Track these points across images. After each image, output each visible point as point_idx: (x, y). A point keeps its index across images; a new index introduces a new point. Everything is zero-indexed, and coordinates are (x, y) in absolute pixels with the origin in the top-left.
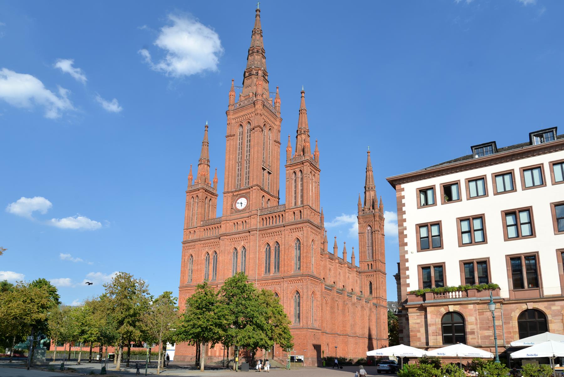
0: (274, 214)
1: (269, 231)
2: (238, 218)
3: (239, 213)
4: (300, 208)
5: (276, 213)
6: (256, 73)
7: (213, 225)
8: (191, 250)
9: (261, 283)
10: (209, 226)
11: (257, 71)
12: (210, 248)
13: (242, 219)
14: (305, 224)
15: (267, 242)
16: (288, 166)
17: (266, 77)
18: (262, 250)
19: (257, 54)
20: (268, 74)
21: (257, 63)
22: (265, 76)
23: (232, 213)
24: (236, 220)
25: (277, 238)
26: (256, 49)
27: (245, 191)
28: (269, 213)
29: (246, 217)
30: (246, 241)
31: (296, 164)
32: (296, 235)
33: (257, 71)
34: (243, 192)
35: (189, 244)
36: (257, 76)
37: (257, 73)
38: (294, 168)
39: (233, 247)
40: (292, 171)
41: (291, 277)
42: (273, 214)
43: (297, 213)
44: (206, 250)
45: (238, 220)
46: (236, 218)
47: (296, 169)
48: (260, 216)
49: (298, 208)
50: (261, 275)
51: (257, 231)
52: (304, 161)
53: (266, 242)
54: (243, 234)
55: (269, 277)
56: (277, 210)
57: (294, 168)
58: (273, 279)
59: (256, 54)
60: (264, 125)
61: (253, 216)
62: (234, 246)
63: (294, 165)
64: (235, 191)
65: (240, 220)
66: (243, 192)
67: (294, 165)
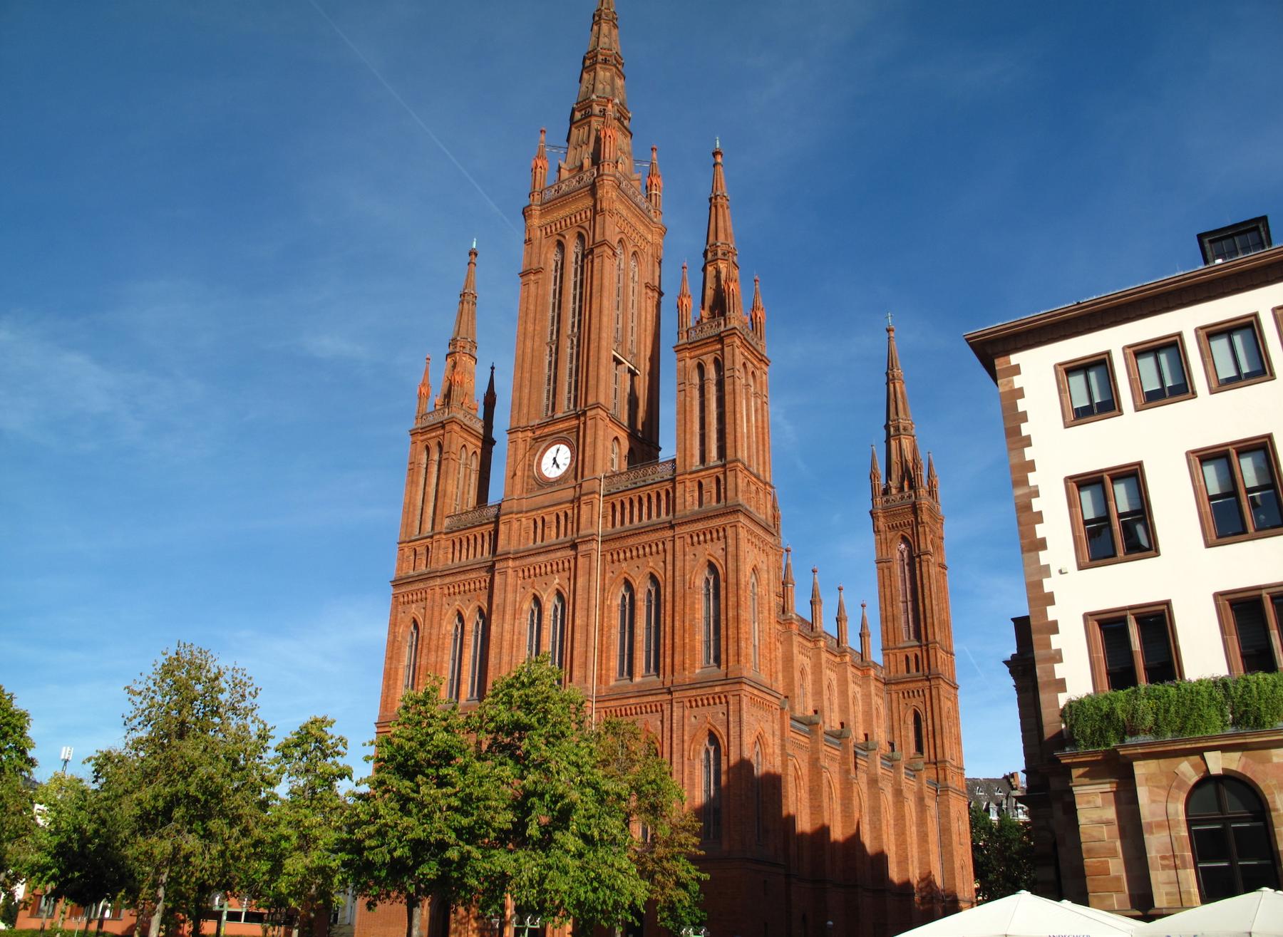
0: (644, 488)
1: (631, 542)
2: (547, 504)
3: (549, 490)
4: (716, 470)
5: (650, 487)
6: (600, 111)
7: (477, 529)
8: (414, 606)
9: (608, 708)
10: (467, 531)
11: (602, 108)
12: (468, 596)
13: (555, 508)
14: (732, 518)
15: (626, 576)
16: (681, 348)
17: (626, 123)
18: (611, 602)
19: (604, 66)
20: (630, 115)
21: (604, 89)
22: (622, 119)
24: (539, 512)
25: (654, 564)
26: (602, 55)
27: (567, 424)
28: (630, 486)
29: (567, 502)
31: (705, 342)
32: (707, 553)
33: (602, 108)
34: (561, 426)
35: (410, 588)
36: (603, 119)
37: (603, 113)
38: (698, 352)
40: (695, 362)
41: (693, 686)
42: (641, 489)
43: (710, 485)
44: (457, 603)
45: (545, 510)
46: (540, 505)
47: (704, 357)
48: (607, 498)
49: (712, 471)
50: (607, 682)
51: (598, 541)
52: (726, 334)
53: (622, 577)
54: (559, 554)
55: (630, 689)
56: (652, 477)
57: (698, 352)
58: (641, 694)
59: (601, 68)
60: (620, 241)
62: (533, 591)
63: (698, 344)
64: (540, 426)
65: (551, 509)
66: (561, 426)
67: (698, 344)
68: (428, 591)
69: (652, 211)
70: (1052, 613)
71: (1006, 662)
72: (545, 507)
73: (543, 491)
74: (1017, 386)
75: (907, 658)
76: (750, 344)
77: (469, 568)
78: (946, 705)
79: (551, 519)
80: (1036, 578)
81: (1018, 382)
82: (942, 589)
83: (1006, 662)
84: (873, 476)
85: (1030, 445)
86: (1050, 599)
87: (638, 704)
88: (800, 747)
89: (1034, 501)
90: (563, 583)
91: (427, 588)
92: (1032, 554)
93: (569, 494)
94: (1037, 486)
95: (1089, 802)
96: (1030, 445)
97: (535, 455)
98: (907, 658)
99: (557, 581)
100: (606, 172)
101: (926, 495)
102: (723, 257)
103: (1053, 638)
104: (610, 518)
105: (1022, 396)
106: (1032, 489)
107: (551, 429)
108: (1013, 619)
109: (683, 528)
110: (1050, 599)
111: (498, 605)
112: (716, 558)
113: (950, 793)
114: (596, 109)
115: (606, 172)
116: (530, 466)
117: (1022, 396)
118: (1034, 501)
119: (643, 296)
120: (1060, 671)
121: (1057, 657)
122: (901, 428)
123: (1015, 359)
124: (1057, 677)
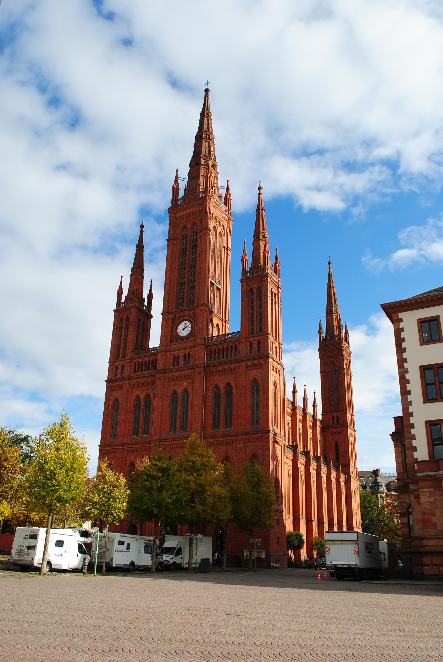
5: (228, 343)
6: (204, 163)
13: (184, 350)
16: (243, 281)
23: (172, 342)
24: (177, 352)
29: (190, 348)
30: (190, 381)
39: (172, 389)
42: (224, 344)
44: (138, 392)
45: (179, 351)
47: (254, 285)
61: (199, 347)
62: (174, 388)
65: (183, 351)
68: (124, 385)
69: (227, 211)
70: (412, 420)
71: (390, 435)
72: (180, 350)
73: (178, 342)
74: (401, 327)
75: (333, 417)
76: (274, 280)
77: (143, 376)
78: (350, 439)
79: (181, 355)
80: (406, 406)
81: (401, 325)
82: (350, 386)
83: (390, 435)
84: (320, 332)
85: (405, 352)
86: (411, 414)
87: (222, 440)
88: (290, 459)
89: (406, 375)
90: (188, 385)
91: (123, 384)
92: (405, 396)
93: (190, 344)
94: (408, 369)
95: (424, 495)
96: (405, 352)
97: (175, 325)
98: (333, 417)
99: (185, 384)
100: (208, 194)
101: (344, 342)
102: (262, 239)
103: (412, 430)
104: (209, 356)
105: (403, 331)
106: (406, 370)
107: (182, 314)
108: (393, 417)
109: (243, 363)
110: (411, 414)
111: (157, 394)
112: (258, 377)
113: (351, 479)
114: (203, 162)
115: (208, 194)
116: (172, 330)
117: (403, 331)
118: (406, 375)
119: (223, 252)
120: (414, 443)
121: (414, 437)
122: (333, 310)
123: (401, 315)
124: (413, 445)
